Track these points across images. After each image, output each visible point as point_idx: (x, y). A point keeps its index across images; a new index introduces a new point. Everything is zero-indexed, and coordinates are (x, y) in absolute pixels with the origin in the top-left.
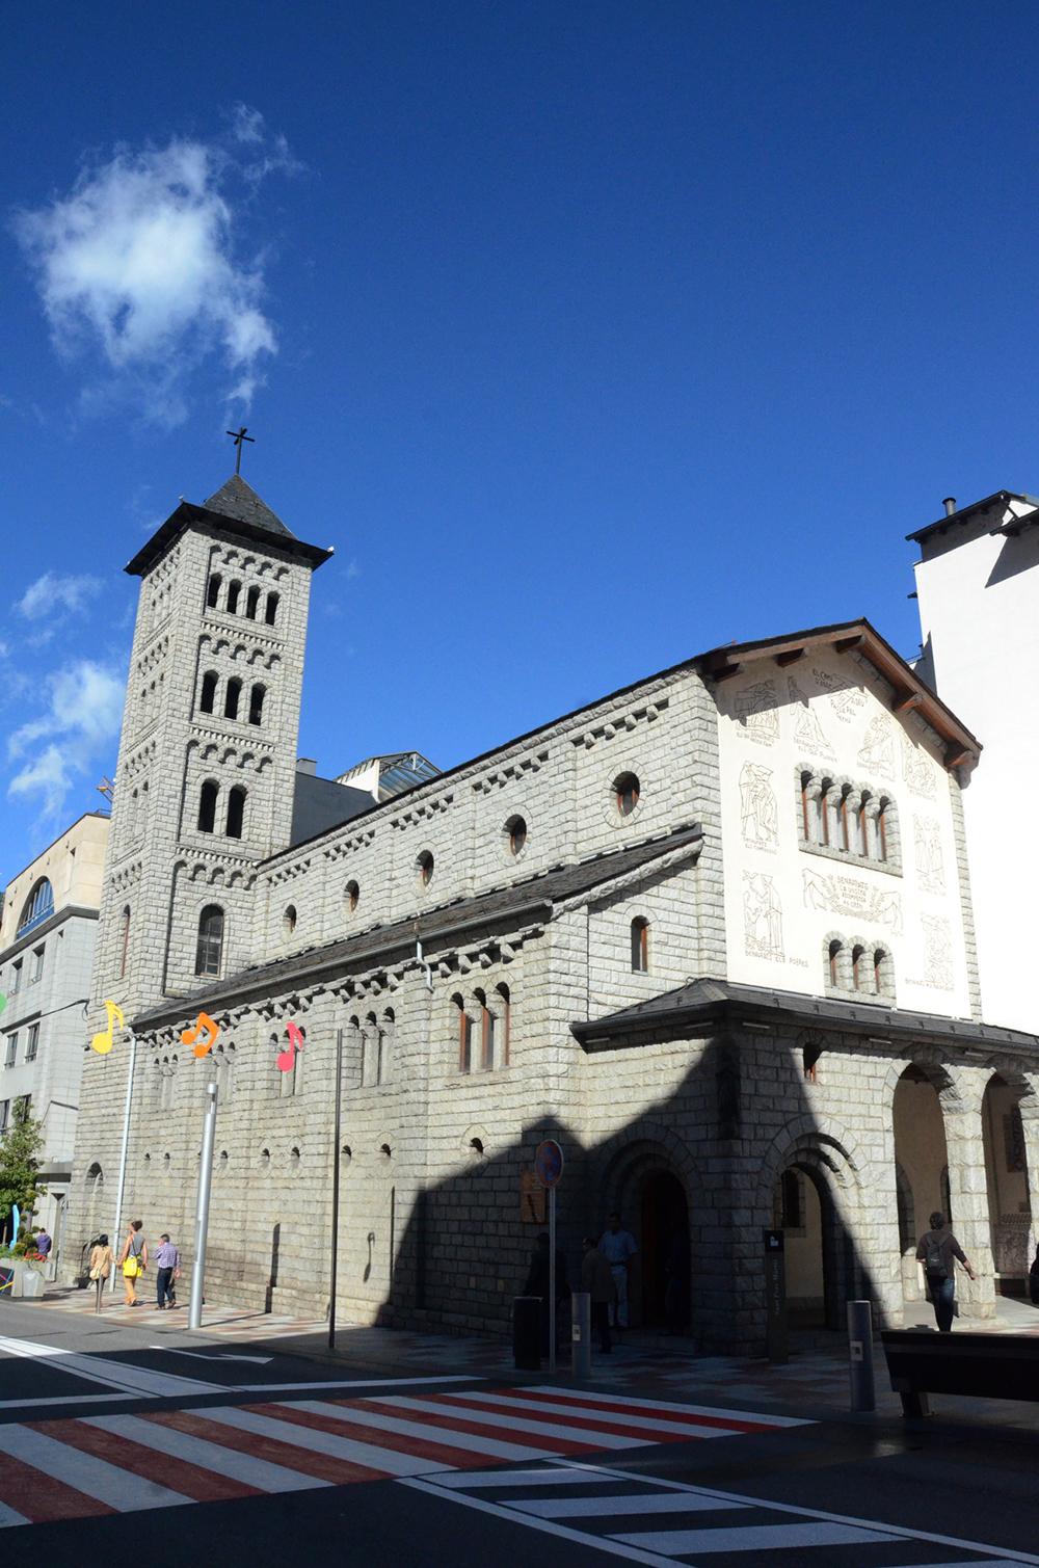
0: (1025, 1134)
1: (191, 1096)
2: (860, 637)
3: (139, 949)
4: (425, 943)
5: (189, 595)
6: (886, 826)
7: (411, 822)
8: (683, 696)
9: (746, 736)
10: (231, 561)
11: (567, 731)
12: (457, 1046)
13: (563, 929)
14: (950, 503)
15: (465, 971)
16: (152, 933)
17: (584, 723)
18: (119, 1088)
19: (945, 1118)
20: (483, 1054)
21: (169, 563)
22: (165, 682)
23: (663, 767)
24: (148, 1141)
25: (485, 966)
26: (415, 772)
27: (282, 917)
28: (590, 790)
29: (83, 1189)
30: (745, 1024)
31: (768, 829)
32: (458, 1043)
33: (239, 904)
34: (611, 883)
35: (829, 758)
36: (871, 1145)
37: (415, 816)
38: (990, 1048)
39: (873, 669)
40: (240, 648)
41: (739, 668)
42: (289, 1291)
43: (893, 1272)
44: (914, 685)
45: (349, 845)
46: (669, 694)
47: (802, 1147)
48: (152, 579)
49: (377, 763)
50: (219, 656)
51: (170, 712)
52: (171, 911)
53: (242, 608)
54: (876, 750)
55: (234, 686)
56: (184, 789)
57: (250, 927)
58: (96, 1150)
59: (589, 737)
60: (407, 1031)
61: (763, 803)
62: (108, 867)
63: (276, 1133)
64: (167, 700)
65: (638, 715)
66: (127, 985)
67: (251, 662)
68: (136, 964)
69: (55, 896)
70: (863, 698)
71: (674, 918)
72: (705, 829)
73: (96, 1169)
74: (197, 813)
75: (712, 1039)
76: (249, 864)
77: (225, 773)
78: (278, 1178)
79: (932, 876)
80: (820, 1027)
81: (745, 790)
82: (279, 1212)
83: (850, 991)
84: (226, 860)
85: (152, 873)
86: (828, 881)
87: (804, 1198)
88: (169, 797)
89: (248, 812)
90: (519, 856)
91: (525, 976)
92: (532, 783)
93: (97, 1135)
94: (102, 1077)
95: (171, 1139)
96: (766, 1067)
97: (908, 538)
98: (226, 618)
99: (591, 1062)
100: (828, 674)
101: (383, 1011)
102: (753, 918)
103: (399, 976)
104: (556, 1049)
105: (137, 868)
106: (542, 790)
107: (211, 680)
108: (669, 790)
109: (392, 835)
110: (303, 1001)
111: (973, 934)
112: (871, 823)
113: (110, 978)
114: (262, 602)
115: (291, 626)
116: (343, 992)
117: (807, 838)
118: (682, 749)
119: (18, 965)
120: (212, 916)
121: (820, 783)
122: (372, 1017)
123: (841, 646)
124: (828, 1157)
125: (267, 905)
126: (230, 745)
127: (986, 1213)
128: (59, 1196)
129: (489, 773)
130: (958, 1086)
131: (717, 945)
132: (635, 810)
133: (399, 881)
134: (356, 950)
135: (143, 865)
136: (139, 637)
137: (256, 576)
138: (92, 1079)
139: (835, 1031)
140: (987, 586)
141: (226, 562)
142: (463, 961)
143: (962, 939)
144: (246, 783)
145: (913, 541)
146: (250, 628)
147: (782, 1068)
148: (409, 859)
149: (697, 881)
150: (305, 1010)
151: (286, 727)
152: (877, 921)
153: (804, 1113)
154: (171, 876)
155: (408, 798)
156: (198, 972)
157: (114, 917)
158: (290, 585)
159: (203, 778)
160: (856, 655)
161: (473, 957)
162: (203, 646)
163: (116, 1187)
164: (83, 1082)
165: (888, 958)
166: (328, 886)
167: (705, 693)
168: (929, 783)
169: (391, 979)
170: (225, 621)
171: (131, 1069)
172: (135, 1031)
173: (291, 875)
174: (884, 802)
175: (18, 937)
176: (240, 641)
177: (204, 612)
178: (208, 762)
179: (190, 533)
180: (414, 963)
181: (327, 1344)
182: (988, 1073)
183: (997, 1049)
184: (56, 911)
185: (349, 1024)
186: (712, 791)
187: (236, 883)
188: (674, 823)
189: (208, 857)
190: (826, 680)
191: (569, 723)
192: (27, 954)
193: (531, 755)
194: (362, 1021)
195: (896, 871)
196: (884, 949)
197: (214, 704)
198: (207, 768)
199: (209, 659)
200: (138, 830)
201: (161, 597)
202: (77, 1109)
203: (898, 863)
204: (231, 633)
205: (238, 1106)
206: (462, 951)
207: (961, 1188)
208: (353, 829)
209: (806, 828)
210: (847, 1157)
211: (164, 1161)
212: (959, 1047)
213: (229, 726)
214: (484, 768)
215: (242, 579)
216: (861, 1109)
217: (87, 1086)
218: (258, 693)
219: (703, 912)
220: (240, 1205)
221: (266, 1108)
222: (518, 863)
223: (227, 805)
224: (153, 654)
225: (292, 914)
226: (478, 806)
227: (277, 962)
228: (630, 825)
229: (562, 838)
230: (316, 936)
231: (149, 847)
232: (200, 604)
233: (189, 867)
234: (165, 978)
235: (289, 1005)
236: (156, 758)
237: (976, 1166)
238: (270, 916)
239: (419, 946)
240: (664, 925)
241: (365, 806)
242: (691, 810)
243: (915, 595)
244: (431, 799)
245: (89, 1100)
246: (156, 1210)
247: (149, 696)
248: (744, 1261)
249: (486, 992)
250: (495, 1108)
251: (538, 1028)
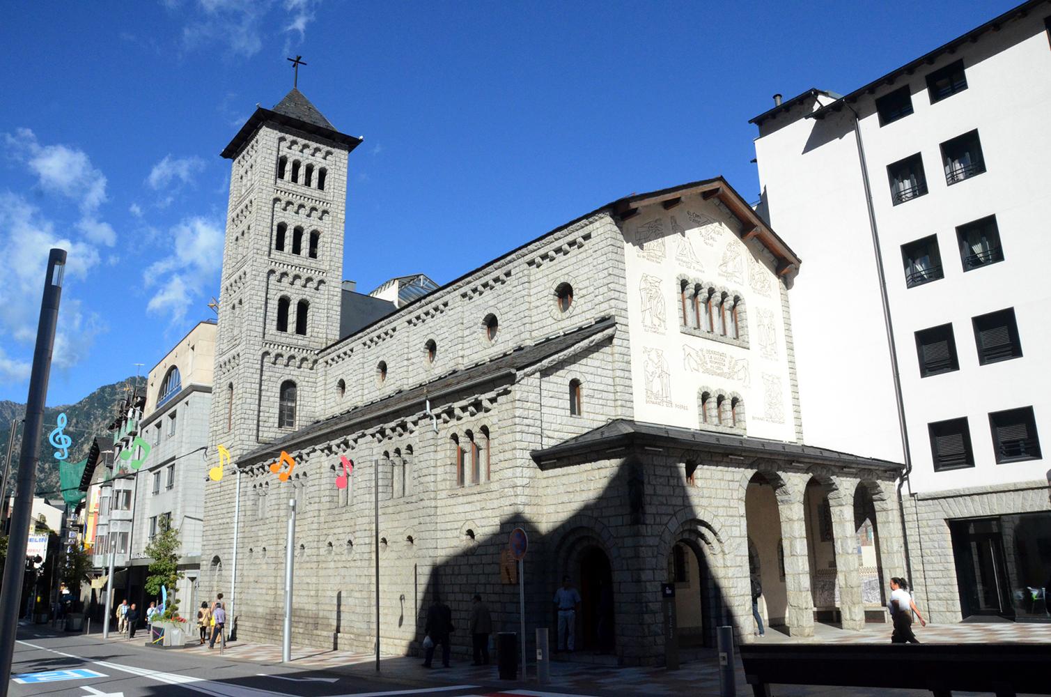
0: (832, 516)
1: (279, 509)
2: (719, 189)
3: (240, 412)
4: (431, 401)
5: (265, 171)
6: (738, 315)
7: (421, 320)
8: (601, 231)
9: (644, 257)
10: (293, 147)
11: (523, 257)
12: (455, 469)
13: (524, 388)
14: (778, 98)
15: (459, 418)
16: (248, 400)
17: (535, 251)
18: (230, 505)
19: (780, 507)
20: (473, 474)
21: (251, 150)
22: (251, 231)
23: (588, 279)
24: (251, 540)
25: (472, 414)
26: (422, 288)
27: (335, 387)
28: (540, 295)
29: (208, 573)
30: (646, 448)
31: (659, 319)
32: (456, 467)
33: (307, 379)
34: (555, 357)
35: (700, 271)
36: (732, 526)
37: (423, 316)
38: (807, 460)
39: (728, 211)
40: (301, 206)
41: (638, 211)
42: (349, 635)
43: (747, 608)
44: (755, 221)
45: (379, 337)
46: (591, 229)
47: (686, 528)
48: (239, 161)
49: (397, 282)
50: (287, 212)
51: (255, 251)
52: (261, 385)
53: (301, 179)
54: (730, 264)
55: (298, 232)
56: (266, 303)
57: (314, 395)
58: (216, 547)
59: (538, 260)
60: (422, 460)
61: (655, 302)
62: (217, 357)
63: (336, 531)
64: (253, 243)
65: (571, 244)
66: (233, 436)
67: (309, 216)
68: (239, 422)
69: (182, 378)
70: (721, 230)
71: (598, 379)
72: (617, 319)
73: (217, 560)
74: (276, 319)
75: (624, 459)
76: (312, 352)
77: (294, 291)
78: (339, 561)
79: (769, 348)
80: (696, 448)
81: (643, 293)
82: (340, 583)
83: (716, 425)
84: (297, 350)
85: (246, 360)
86: (700, 353)
87: (688, 563)
88: (256, 308)
89: (311, 317)
90: (493, 341)
91: (499, 421)
92: (501, 292)
93: (216, 537)
94: (219, 498)
95: (266, 538)
96: (661, 476)
97: (750, 122)
98: (291, 186)
99: (545, 476)
100: (698, 214)
101: (405, 447)
103: (415, 423)
104: (521, 468)
105: (236, 358)
106: (508, 296)
107: (282, 228)
108: (593, 294)
109: (408, 330)
110: (351, 443)
111: (797, 386)
112: (728, 314)
113: (221, 432)
114: (315, 175)
115: (335, 191)
116: (378, 435)
117: (685, 324)
118: (601, 266)
119: (159, 426)
120: (288, 388)
121: (694, 287)
122: (398, 451)
123: (706, 195)
124: (703, 534)
125: (325, 380)
126: (297, 272)
127: (807, 568)
128: (193, 579)
129: (472, 286)
130: (788, 486)
131: (627, 397)
132: (571, 308)
133: (414, 360)
134: (386, 406)
135: (241, 355)
136: (232, 200)
137: (310, 157)
138: (211, 500)
139: (706, 452)
140: (803, 154)
141: (290, 148)
142: (457, 412)
144: (308, 298)
145: (753, 123)
147: (672, 476)
148: (419, 345)
149: (612, 354)
150: (353, 448)
151: (335, 259)
152: (733, 379)
153: (687, 505)
154: (260, 362)
155: (418, 304)
156: (280, 426)
157: (222, 391)
158: (334, 163)
159: (279, 295)
160: (716, 201)
161: (464, 409)
162: (276, 205)
163: (230, 571)
164: (206, 502)
165: (741, 403)
166: (366, 365)
167: (616, 228)
168: (767, 286)
169: (410, 426)
170: (290, 188)
171: (238, 492)
172: (239, 467)
173: (341, 359)
174: (737, 299)
175: (158, 407)
176: (301, 201)
177: (276, 182)
178: (282, 284)
179: (264, 128)
180: (425, 414)
181: (375, 668)
182: (807, 477)
183: (812, 461)
184: (183, 388)
185: (382, 457)
187: (304, 365)
188: (596, 316)
189: (284, 348)
190: (696, 219)
191: (524, 250)
192: (165, 418)
193: (499, 273)
194: (392, 454)
195: (745, 345)
197: (285, 244)
198: (281, 288)
199: (280, 214)
200: (236, 332)
201: (246, 173)
202: (202, 520)
203: (746, 340)
204: (295, 196)
205: (311, 514)
206: (456, 406)
207: (791, 552)
208: (382, 327)
209: (685, 317)
210: (715, 534)
211: (262, 552)
212: (788, 460)
213: (295, 260)
214: (469, 283)
215: (301, 159)
216: (725, 503)
217: (208, 504)
218: (315, 237)
219: (617, 375)
220: (314, 580)
221: (329, 515)
222: (493, 346)
223: (296, 313)
224: (242, 212)
225: (342, 385)
226: (465, 308)
227: (333, 417)
228: (568, 318)
229: (522, 328)
230: (359, 399)
231: (244, 343)
232: (273, 177)
233: (271, 356)
234: (258, 430)
235: (342, 445)
236: (247, 282)
237: (801, 538)
238: (328, 387)
239: (428, 403)
240: (591, 385)
241: (390, 311)
242: (608, 307)
243: (755, 161)
244: (433, 305)
245: (210, 513)
246: (258, 585)
247: (240, 241)
248: (650, 604)
249: (473, 431)
250: (482, 509)
251: (508, 455)
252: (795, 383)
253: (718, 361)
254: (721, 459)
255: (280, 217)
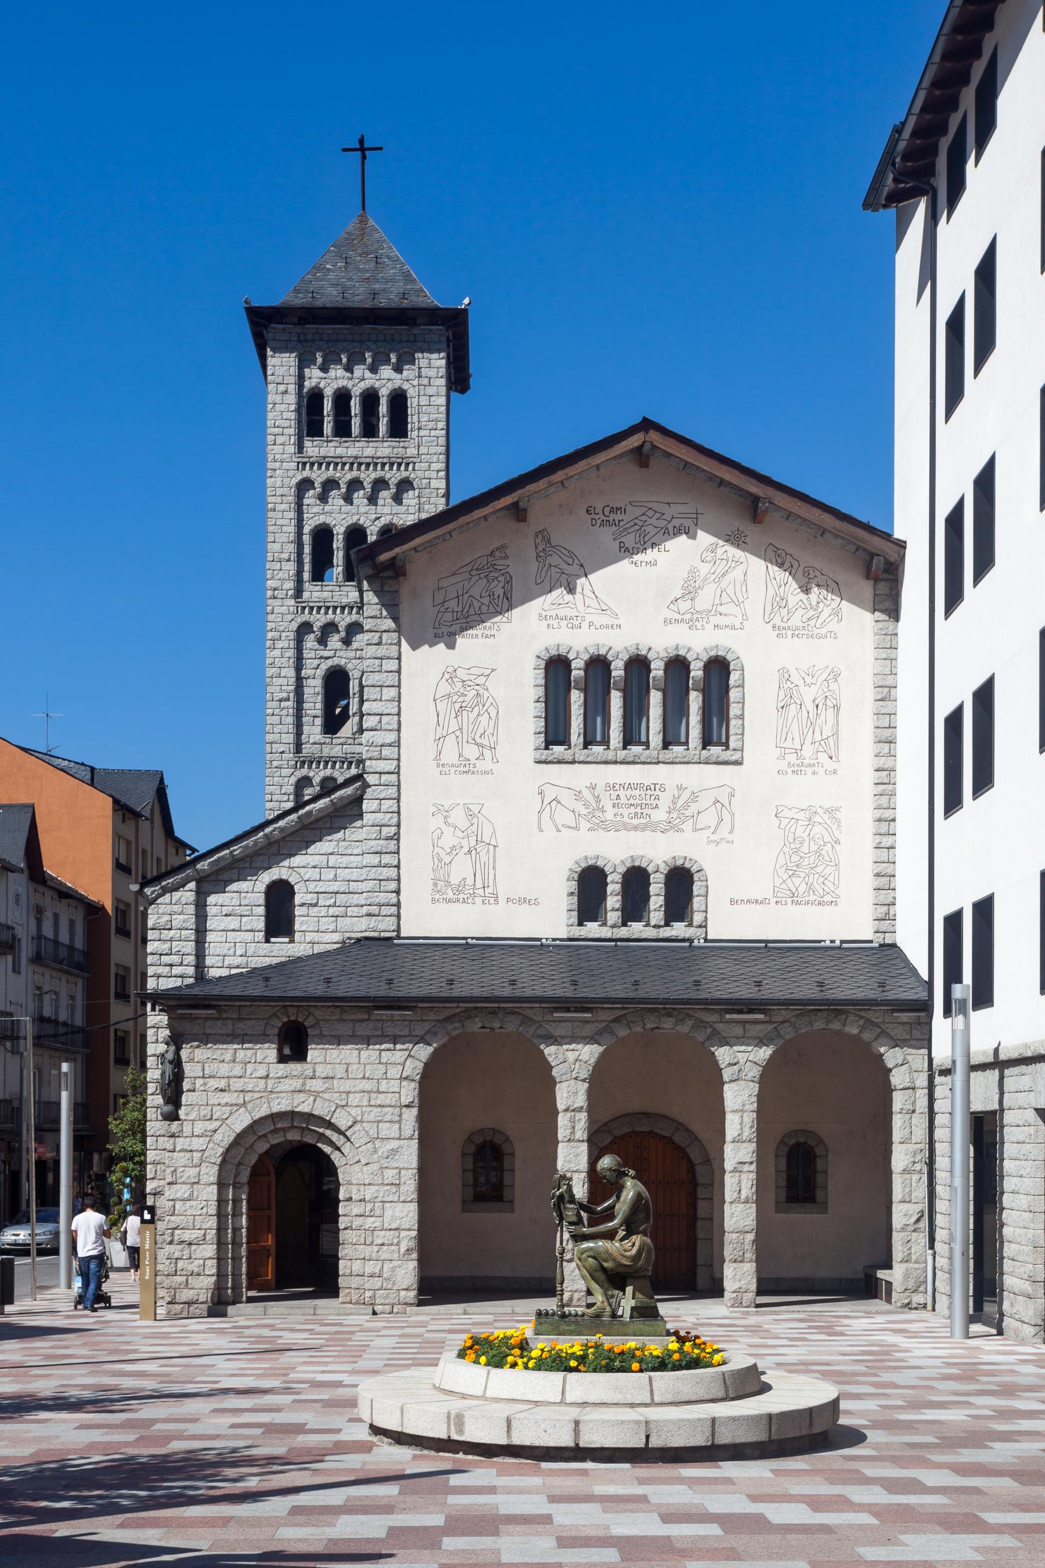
13: (162, 909)
34: (227, 851)
36: (379, 1122)
43: (403, 1250)
47: (279, 1125)
71: (331, 874)
79: (808, 751)
81: (442, 706)
86: (587, 794)
102: (447, 859)
111: (894, 820)
143: (869, 827)
146: (369, 452)
176: (355, 473)
177: (300, 448)
186: (384, 717)
196: (687, 865)
199: (316, 509)
204: (339, 467)
216: (368, 1085)
240: (312, 886)
252: (888, 814)
253: (637, 801)
254: (366, 1017)
255: (315, 515)
